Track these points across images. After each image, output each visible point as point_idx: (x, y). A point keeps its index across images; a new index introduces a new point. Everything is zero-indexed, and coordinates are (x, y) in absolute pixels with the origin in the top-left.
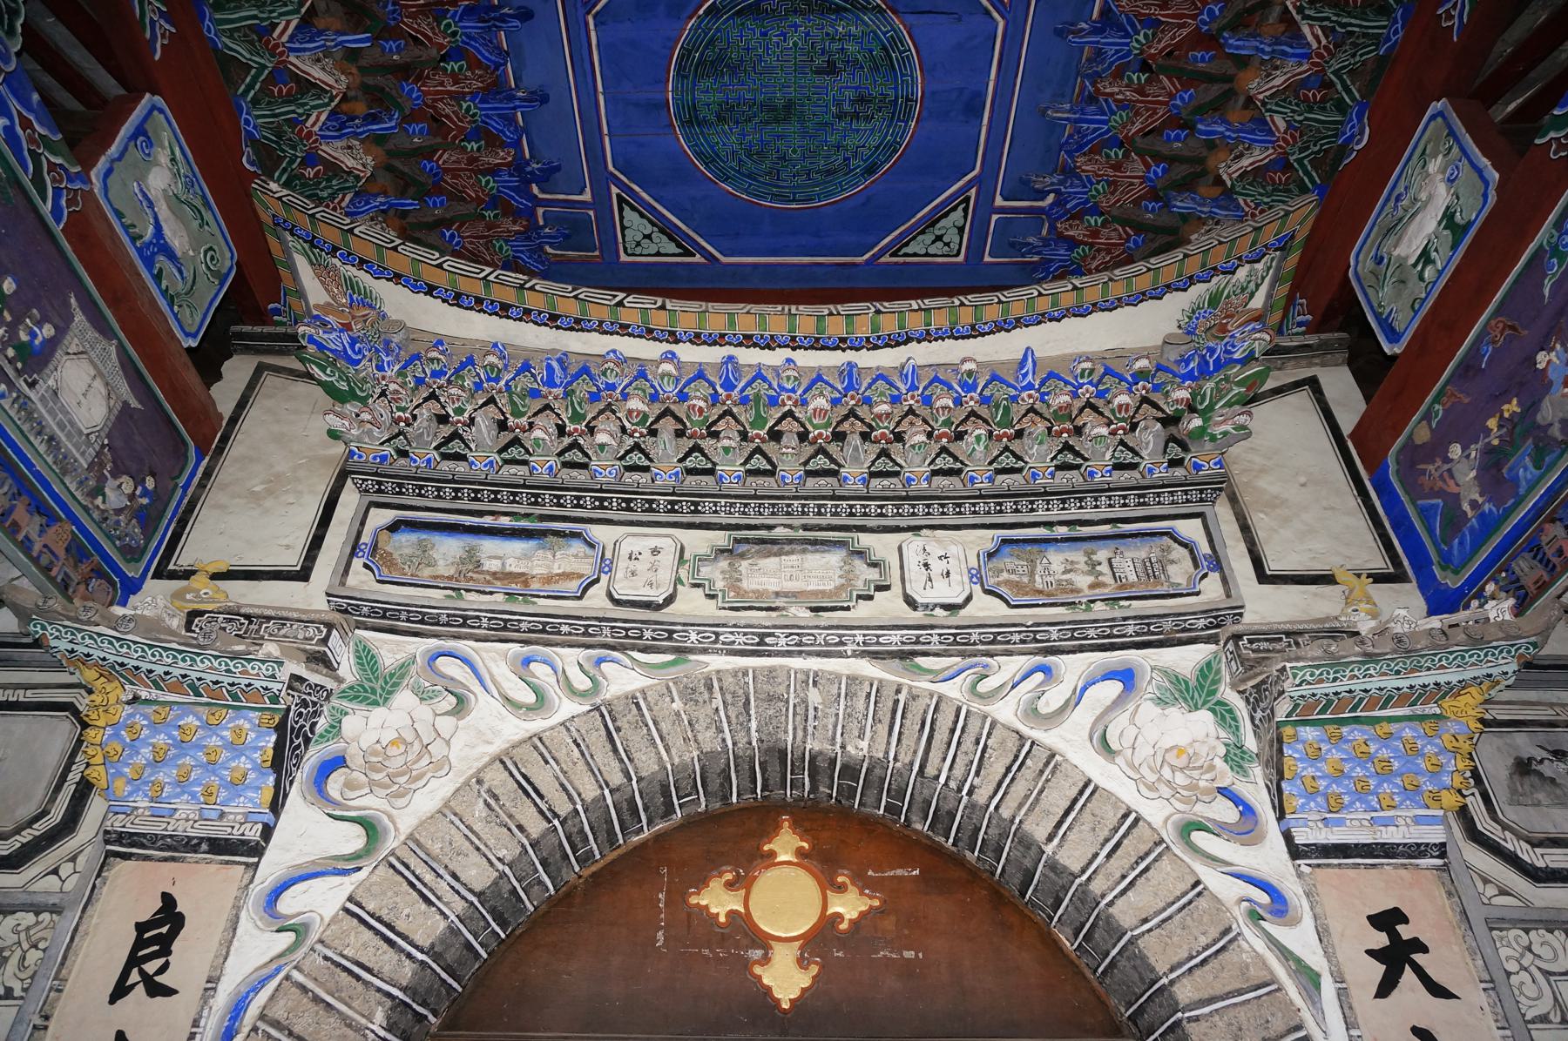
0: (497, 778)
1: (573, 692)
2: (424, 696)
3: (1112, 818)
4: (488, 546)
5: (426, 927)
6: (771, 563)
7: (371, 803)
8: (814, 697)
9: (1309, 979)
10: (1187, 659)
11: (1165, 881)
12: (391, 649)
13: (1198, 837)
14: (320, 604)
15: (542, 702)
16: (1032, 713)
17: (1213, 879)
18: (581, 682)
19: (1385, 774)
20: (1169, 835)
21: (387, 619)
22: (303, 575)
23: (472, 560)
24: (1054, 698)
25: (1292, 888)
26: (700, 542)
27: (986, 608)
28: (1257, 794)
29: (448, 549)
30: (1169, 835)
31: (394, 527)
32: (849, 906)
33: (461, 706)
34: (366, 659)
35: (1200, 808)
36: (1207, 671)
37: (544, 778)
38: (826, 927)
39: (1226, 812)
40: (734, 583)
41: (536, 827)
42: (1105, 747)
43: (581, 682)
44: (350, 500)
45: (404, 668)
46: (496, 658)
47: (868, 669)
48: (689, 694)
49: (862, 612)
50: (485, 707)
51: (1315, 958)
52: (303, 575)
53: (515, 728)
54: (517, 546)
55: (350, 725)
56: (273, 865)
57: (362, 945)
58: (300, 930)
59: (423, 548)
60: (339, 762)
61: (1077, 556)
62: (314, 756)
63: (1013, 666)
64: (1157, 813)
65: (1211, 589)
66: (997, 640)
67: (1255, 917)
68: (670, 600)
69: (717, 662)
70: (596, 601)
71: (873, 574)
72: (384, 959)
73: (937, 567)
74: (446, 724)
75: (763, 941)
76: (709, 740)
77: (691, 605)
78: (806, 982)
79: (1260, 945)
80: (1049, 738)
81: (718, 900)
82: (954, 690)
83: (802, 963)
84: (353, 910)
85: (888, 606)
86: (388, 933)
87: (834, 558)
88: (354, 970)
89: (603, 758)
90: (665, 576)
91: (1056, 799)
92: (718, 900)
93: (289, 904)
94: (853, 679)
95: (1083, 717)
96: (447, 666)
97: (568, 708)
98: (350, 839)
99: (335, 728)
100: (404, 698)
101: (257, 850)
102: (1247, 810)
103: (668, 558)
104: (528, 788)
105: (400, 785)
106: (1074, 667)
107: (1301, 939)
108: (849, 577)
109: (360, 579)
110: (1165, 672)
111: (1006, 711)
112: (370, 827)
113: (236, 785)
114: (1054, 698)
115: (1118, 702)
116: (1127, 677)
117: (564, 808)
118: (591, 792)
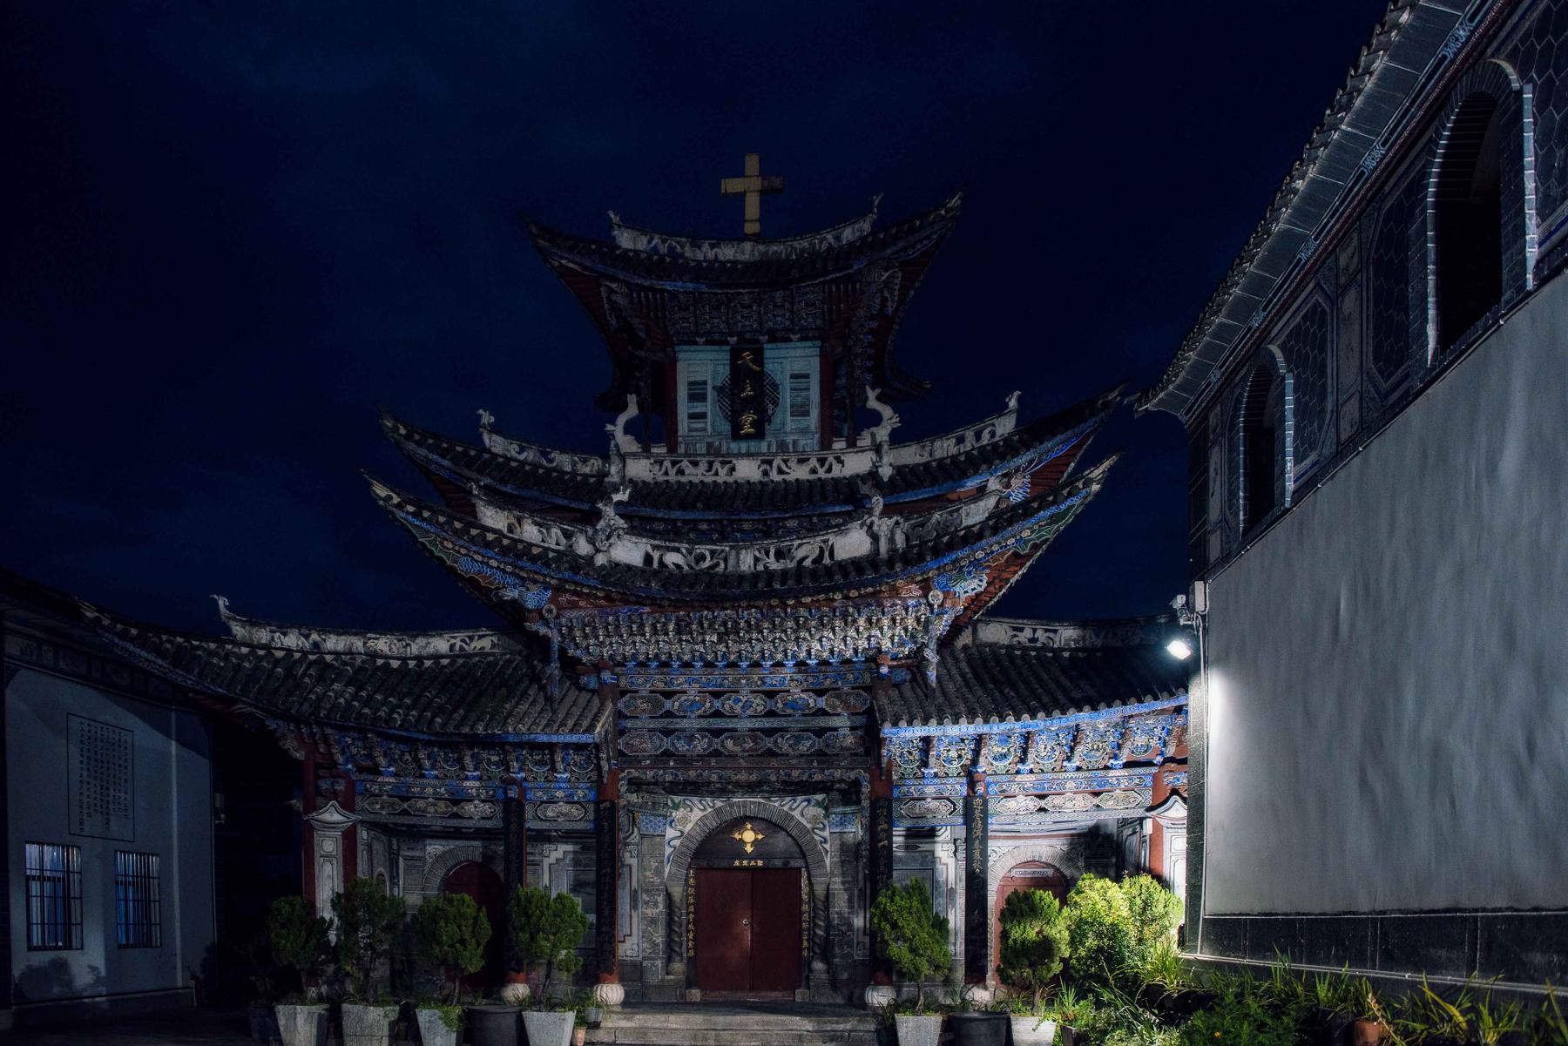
0: (700, 823)
5: (694, 847)
9: (827, 852)
11: (808, 837)
15: (705, 809)
16: (791, 809)
17: (816, 837)
25: (828, 838)
32: (760, 837)
33: (691, 811)
34: (673, 801)
38: (756, 839)
39: (821, 826)
42: (803, 815)
47: (762, 800)
50: (695, 809)
53: (701, 814)
64: (809, 826)
75: (745, 843)
81: (737, 836)
82: (776, 804)
86: (687, 847)
95: (800, 809)
96: (688, 803)
97: (710, 810)
100: (682, 809)
102: (824, 826)
104: (705, 825)
106: (800, 799)
107: (827, 846)
111: (786, 808)
112: (682, 833)
116: (809, 801)
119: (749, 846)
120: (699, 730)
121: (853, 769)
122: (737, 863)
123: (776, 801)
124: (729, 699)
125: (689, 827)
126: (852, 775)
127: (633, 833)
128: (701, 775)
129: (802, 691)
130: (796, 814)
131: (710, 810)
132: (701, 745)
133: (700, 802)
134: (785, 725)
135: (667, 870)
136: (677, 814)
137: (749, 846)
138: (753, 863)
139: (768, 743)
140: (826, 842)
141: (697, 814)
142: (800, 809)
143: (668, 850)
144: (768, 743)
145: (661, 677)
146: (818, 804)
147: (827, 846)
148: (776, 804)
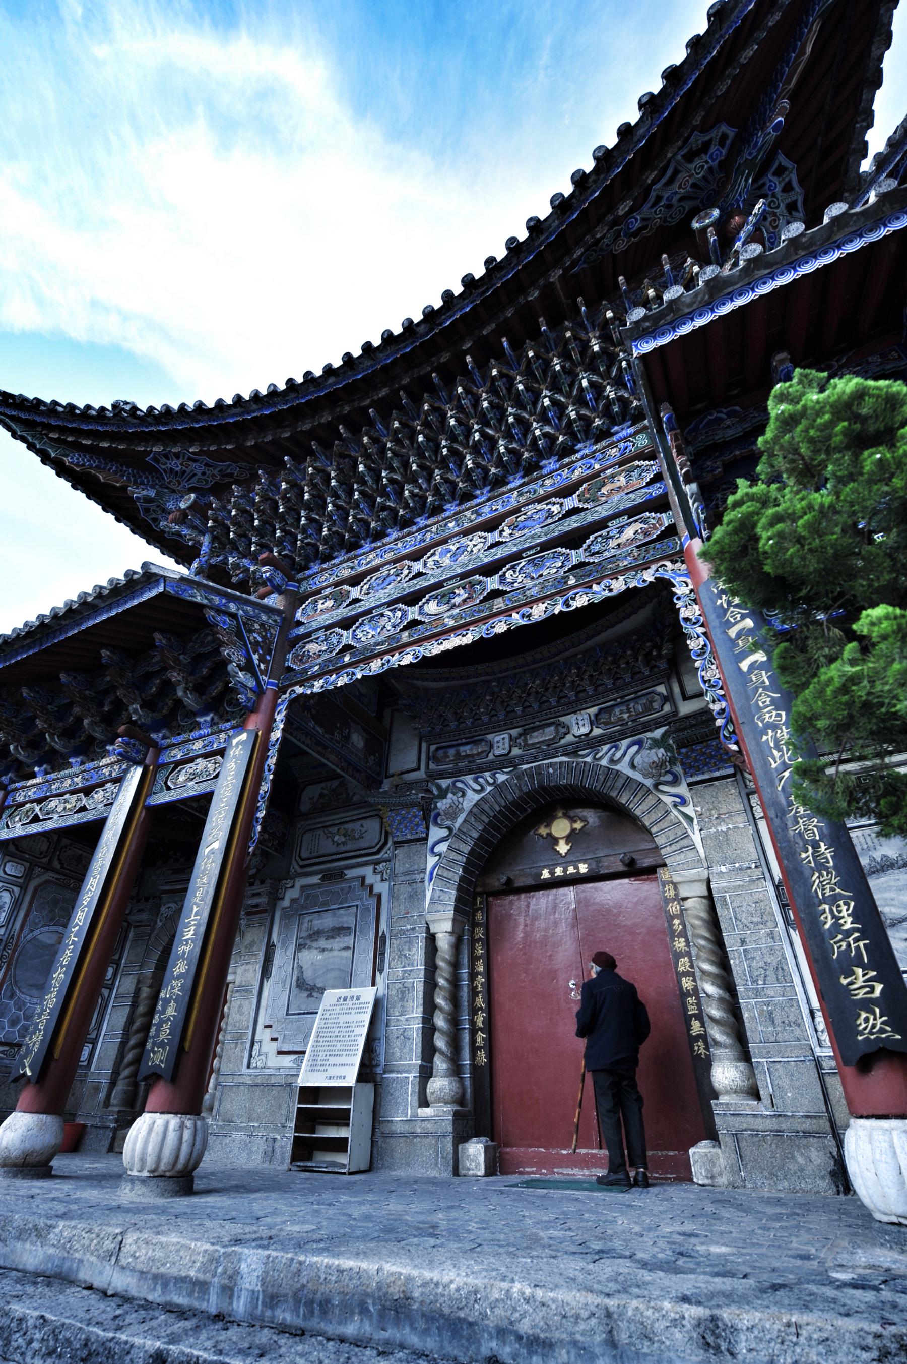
0: (475, 810)
1: (490, 784)
2: (454, 794)
3: (635, 786)
4: (462, 749)
5: (466, 849)
6: (535, 734)
7: (448, 823)
8: (551, 770)
9: (689, 819)
10: (658, 733)
12: (444, 783)
13: (661, 787)
14: (424, 776)
16: (612, 761)
18: (491, 781)
19: (712, 757)
20: (651, 788)
21: (443, 775)
22: (418, 769)
23: (458, 754)
24: (618, 755)
26: (514, 732)
27: (597, 731)
28: (678, 769)
29: (452, 752)
30: (651, 788)
31: (437, 749)
33: (464, 795)
34: (439, 787)
35: (662, 778)
36: (665, 735)
37: (486, 807)
38: (573, 831)
39: (669, 777)
40: (525, 741)
41: (487, 820)
43: (491, 781)
44: (424, 745)
45: (448, 787)
46: (469, 779)
47: (564, 759)
48: (518, 778)
49: (563, 742)
50: (470, 793)
51: (693, 815)
52: (418, 769)
53: (477, 797)
54: (468, 747)
55: (439, 805)
56: (431, 841)
57: (453, 855)
58: (440, 855)
59: (446, 753)
60: (438, 815)
61: (624, 708)
62: (433, 814)
63: (605, 748)
64: (649, 782)
65: (667, 708)
66: (600, 741)
67: (675, 806)
68: (510, 752)
69: (525, 767)
70: (491, 757)
71: (563, 730)
72: (460, 858)
73: (581, 723)
74: (461, 800)
76: (524, 788)
77: (516, 751)
78: (568, 847)
79: (676, 813)
80: (617, 767)
82: (588, 759)
83: (567, 843)
84: (450, 848)
85: (569, 738)
87: (552, 728)
88: (453, 861)
89: (499, 799)
90: (507, 745)
91: (619, 784)
92: (543, 831)
93: (436, 850)
94: (561, 763)
95: (627, 758)
96: (459, 785)
97: (489, 788)
98: (445, 833)
99: (436, 807)
100: (450, 795)
101: (426, 839)
103: (507, 740)
104: (483, 811)
105: (454, 818)
106: (624, 743)
108: (557, 732)
109: (432, 766)
110: (651, 739)
111: (604, 762)
112: (450, 829)
113: (418, 825)
114: (618, 755)
115: (638, 752)
116: (640, 743)
117: (492, 814)
118: (498, 808)
119: (562, 842)
120: (389, 604)
121: (645, 567)
122: (546, 874)
123: (587, 756)
124: (433, 554)
125: (460, 820)
126: (649, 576)
127: (386, 843)
128: (388, 661)
129: (539, 501)
130: (623, 767)
131: (489, 788)
132: (391, 620)
133: (476, 780)
134: (515, 549)
135: (429, 894)
136: (442, 805)
137: (562, 842)
138: (571, 870)
139: (493, 583)
140: (684, 802)
141: (472, 798)
142: (627, 758)
143: (432, 861)
144: (493, 583)
145: (349, 564)
146: (656, 744)
147: (689, 810)
148: (588, 759)
